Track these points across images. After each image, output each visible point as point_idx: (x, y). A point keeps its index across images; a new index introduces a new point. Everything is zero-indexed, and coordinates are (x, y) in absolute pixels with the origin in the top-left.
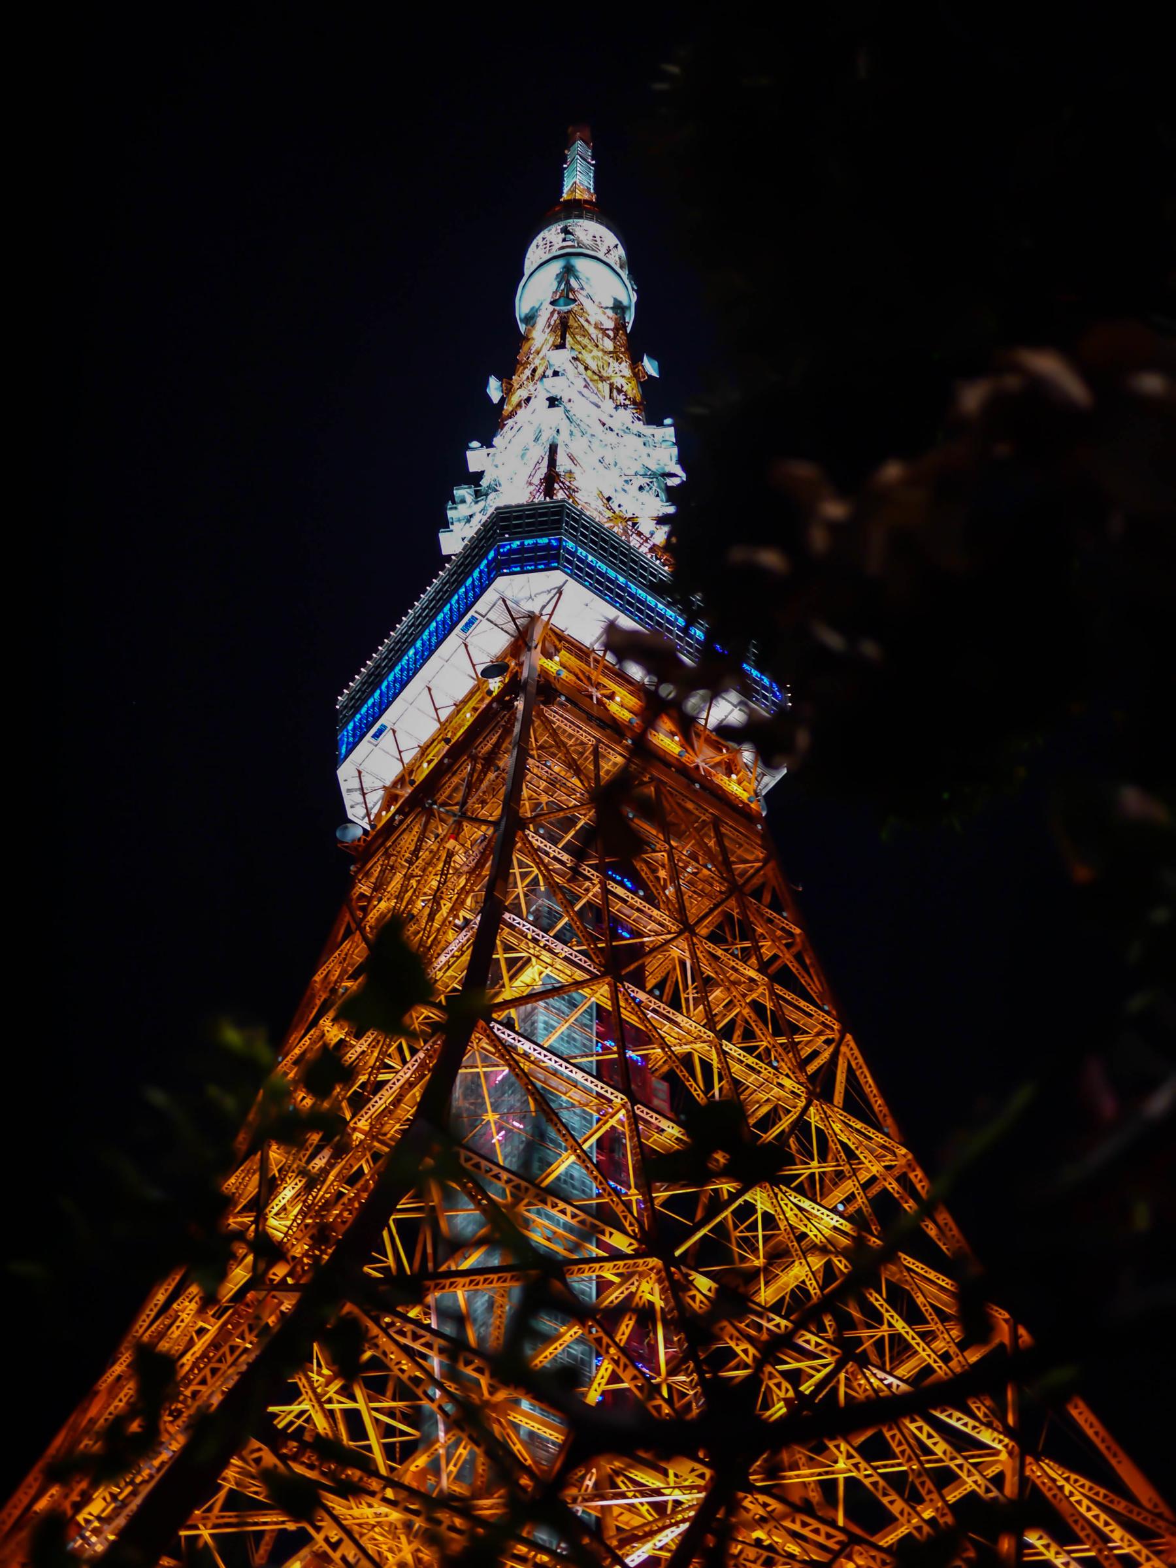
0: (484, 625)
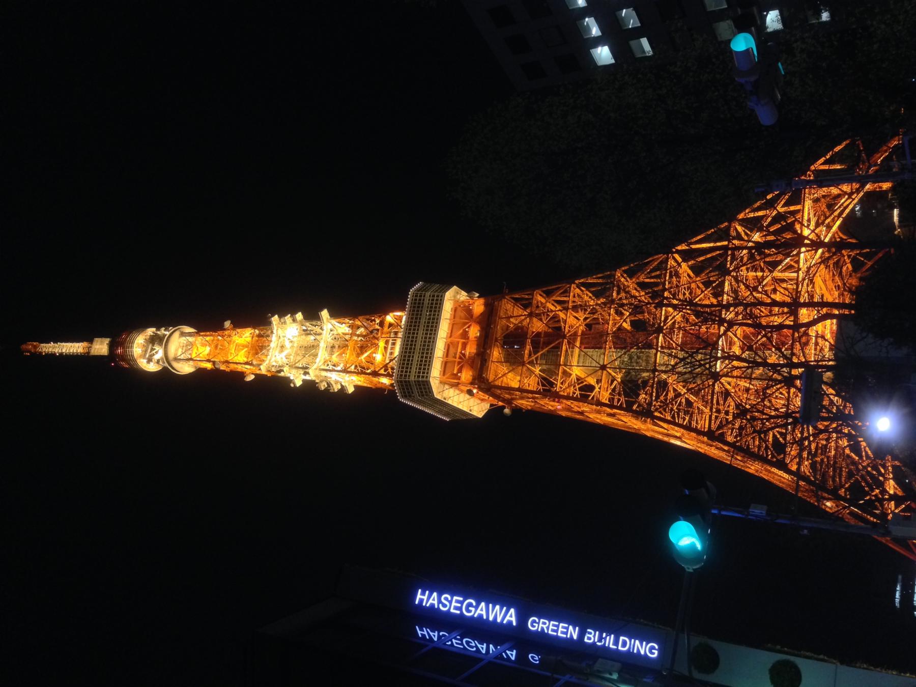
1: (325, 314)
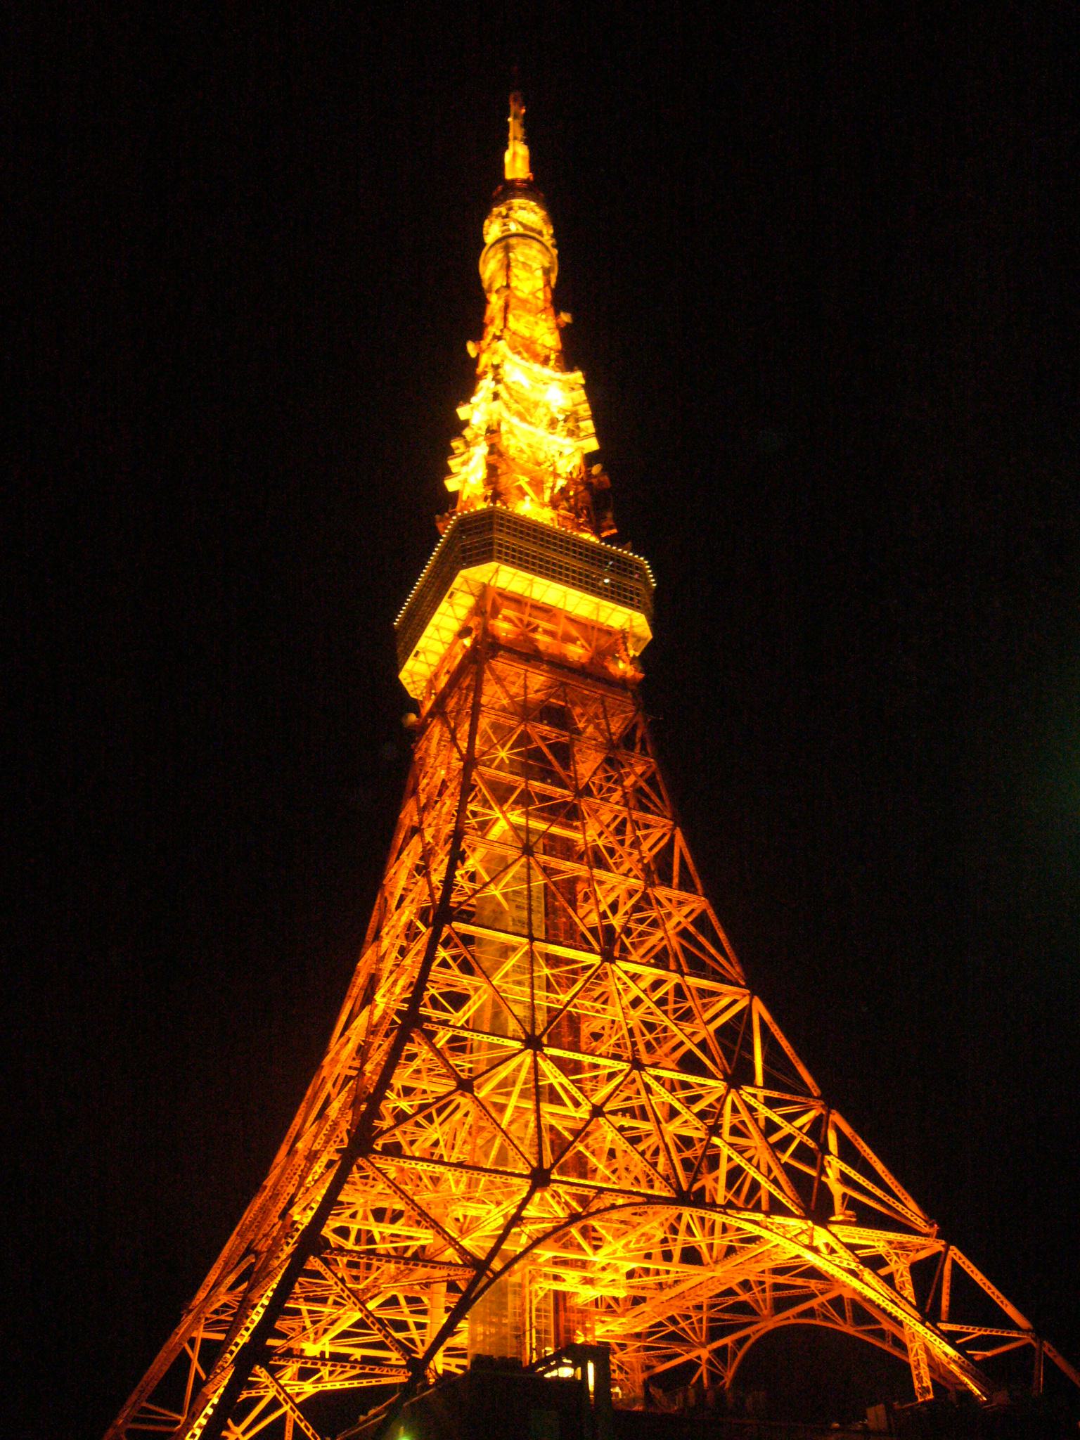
0: (459, 594)
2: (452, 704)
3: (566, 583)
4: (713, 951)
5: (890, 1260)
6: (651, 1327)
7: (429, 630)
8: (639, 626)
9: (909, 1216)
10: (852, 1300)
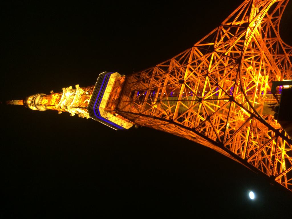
0: (107, 116)
1: (77, 86)
2: (130, 118)
3: (104, 92)
4: (183, 56)
5: (260, 6)
6: (279, 68)
7: (116, 123)
8: (114, 75)
9: (248, 2)
10: (273, 16)
